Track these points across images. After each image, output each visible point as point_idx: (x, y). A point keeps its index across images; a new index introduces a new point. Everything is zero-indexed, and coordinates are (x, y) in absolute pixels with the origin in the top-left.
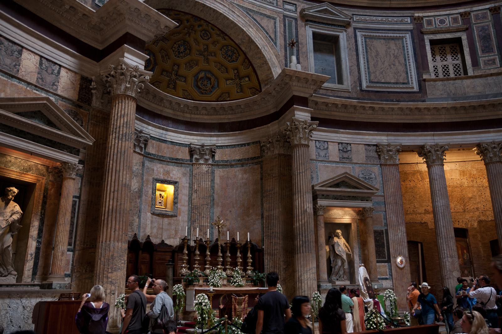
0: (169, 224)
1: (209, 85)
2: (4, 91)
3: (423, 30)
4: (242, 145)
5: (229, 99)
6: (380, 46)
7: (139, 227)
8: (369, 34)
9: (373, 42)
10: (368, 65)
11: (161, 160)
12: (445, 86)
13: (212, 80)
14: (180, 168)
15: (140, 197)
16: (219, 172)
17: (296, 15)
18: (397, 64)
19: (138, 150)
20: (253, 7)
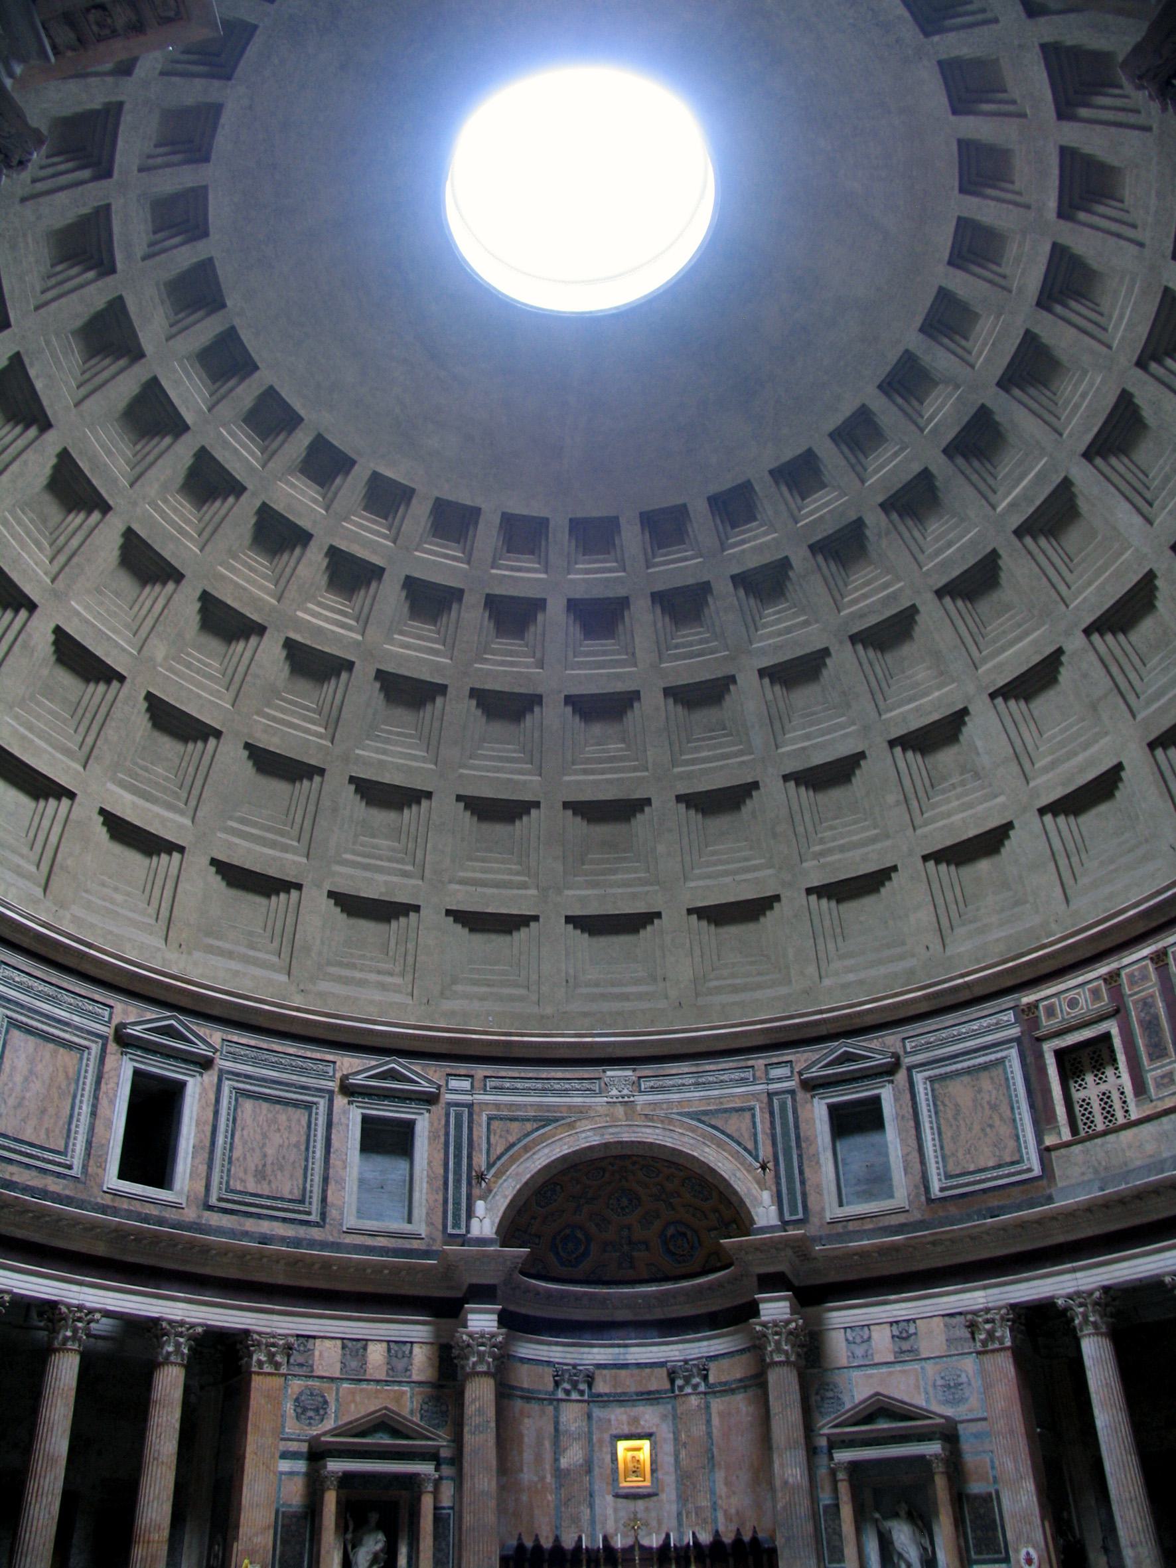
0: (647, 1509)
1: (686, 1245)
2: (354, 1401)
3: (1038, 1034)
4: (742, 1351)
5: (719, 1264)
6: (959, 1090)
7: (593, 1522)
8: (937, 1072)
9: (947, 1087)
10: (941, 1140)
11: (621, 1399)
12: (1087, 1151)
13: (689, 1236)
14: (656, 1407)
15: (589, 1471)
16: (717, 1404)
17: (793, 1083)
18: (997, 1122)
19: (575, 1396)
20: (709, 1104)
